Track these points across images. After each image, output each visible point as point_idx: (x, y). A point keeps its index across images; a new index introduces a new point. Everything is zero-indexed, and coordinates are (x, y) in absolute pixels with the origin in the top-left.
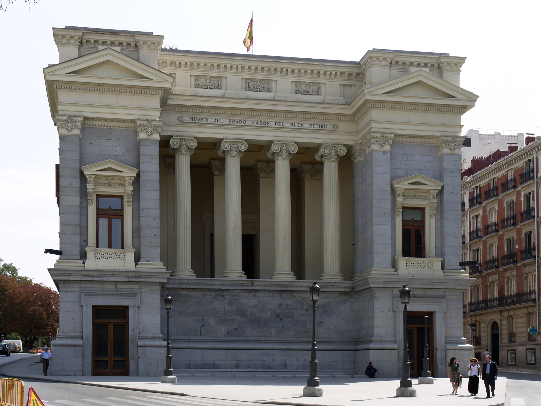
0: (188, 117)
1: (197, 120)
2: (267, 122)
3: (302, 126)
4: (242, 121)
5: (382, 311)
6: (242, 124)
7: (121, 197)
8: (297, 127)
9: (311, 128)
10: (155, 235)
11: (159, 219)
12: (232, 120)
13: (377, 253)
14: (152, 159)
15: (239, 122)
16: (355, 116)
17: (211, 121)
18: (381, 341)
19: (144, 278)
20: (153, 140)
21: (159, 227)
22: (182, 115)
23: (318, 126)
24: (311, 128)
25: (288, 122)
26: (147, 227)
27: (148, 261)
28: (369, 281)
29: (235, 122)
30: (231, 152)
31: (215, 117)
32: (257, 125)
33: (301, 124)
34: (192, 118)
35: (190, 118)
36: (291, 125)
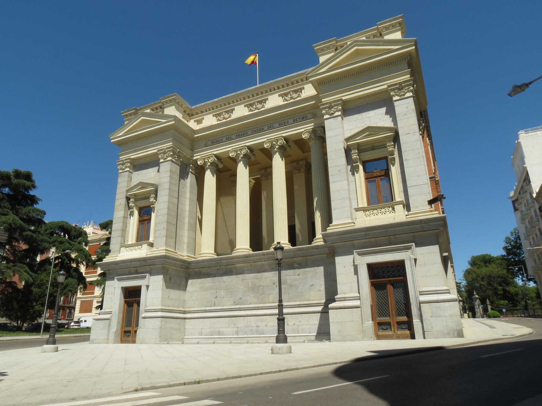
5: (345, 267)
18: (344, 299)
23: (300, 119)
32: (255, 133)
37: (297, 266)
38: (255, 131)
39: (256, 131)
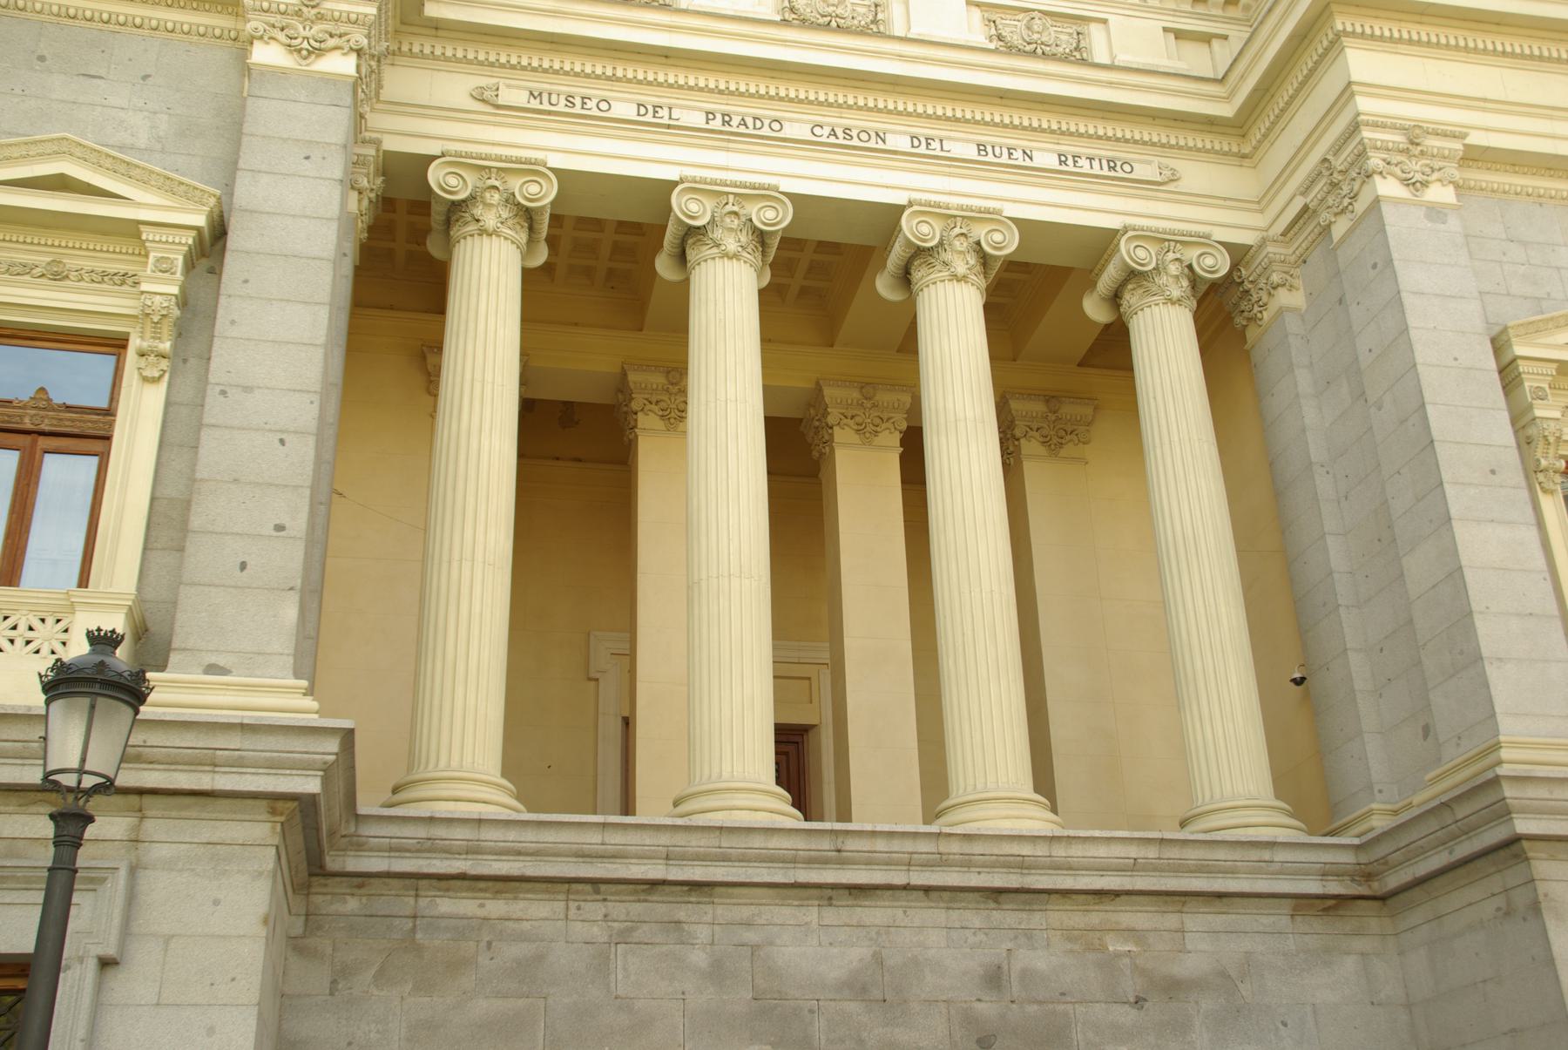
0: (525, 88)
1: (562, 101)
2: (877, 135)
3: (1026, 158)
4: (767, 122)
6: (766, 131)
7: (115, 345)
8: (1005, 159)
9: (1064, 168)
10: (280, 528)
11: (311, 441)
12: (719, 117)
13: (1500, 659)
14: (307, 158)
15: (750, 121)
16: (1243, 136)
17: (624, 109)
19: (172, 762)
20: (322, 79)
21: (308, 483)
22: (494, 81)
23: (1096, 164)
24: (1064, 168)
25: (968, 141)
26: (236, 480)
27: (212, 669)
28: (1504, 799)
29: (735, 122)
30: (717, 234)
31: (642, 99)
32: (832, 140)
33: (1024, 152)
34: (540, 94)
35: (531, 94)
36: (979, 150)
37: (1127, 949)
38: (833, 133)
39: (839, 132)
